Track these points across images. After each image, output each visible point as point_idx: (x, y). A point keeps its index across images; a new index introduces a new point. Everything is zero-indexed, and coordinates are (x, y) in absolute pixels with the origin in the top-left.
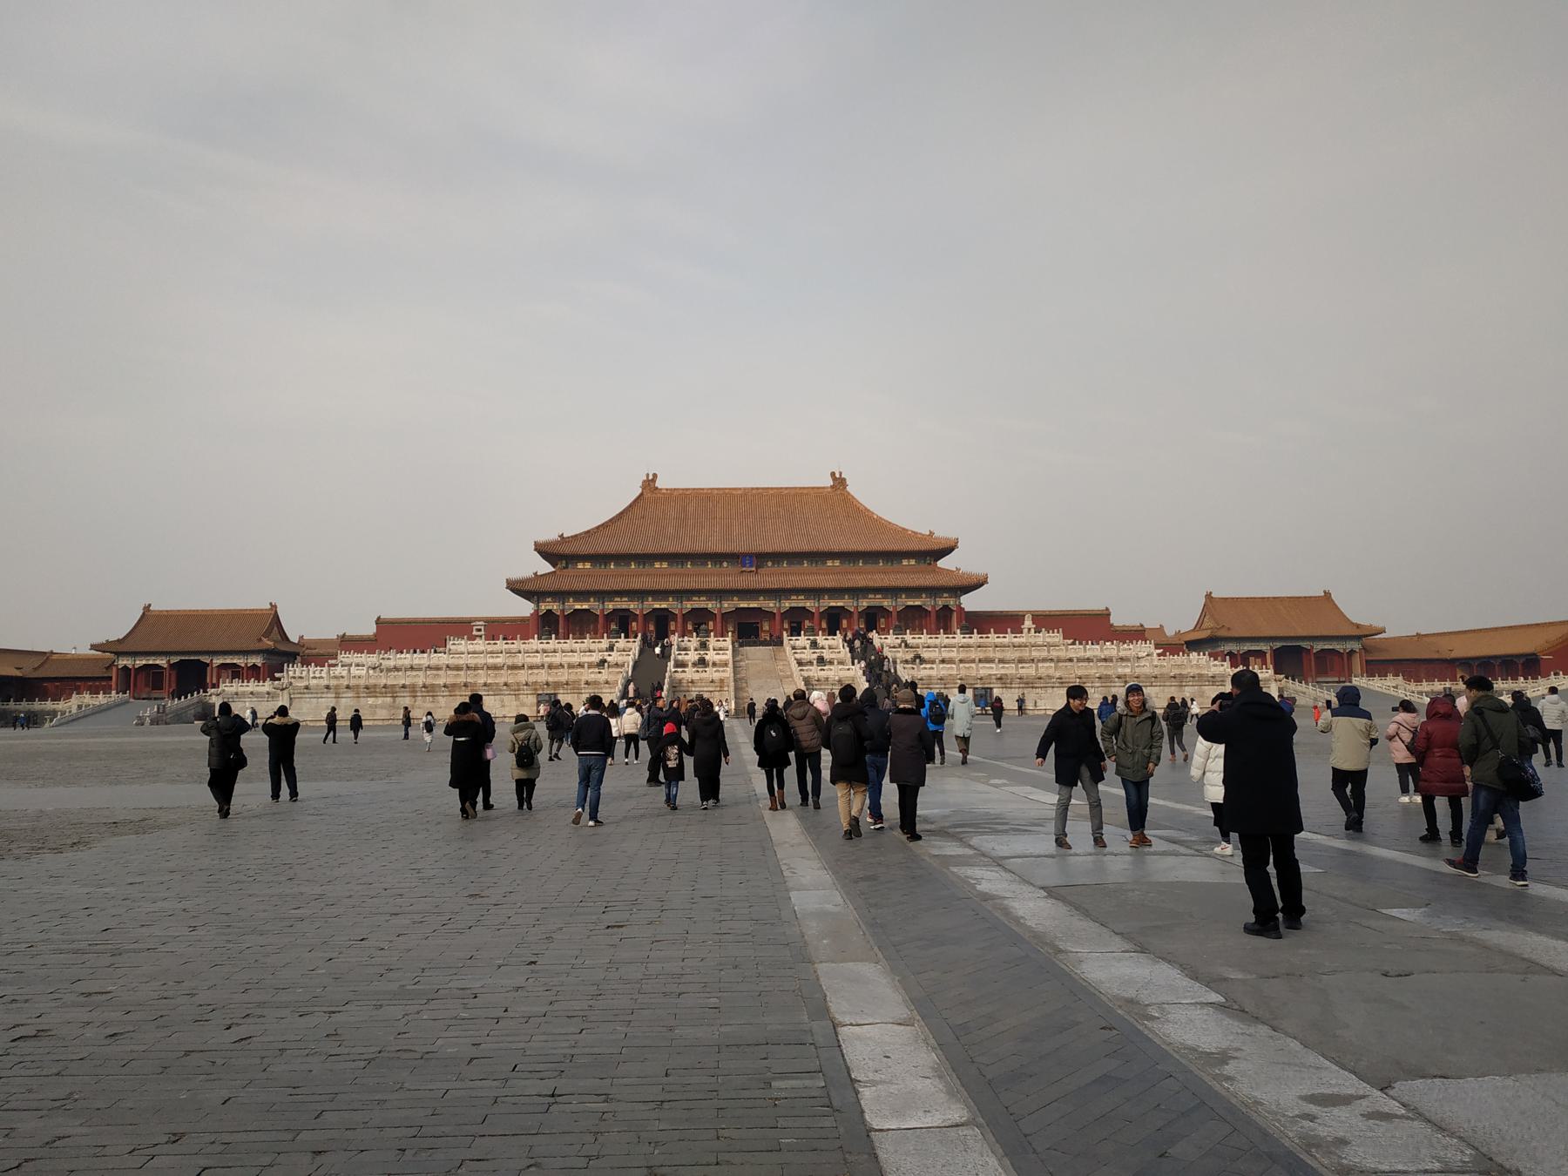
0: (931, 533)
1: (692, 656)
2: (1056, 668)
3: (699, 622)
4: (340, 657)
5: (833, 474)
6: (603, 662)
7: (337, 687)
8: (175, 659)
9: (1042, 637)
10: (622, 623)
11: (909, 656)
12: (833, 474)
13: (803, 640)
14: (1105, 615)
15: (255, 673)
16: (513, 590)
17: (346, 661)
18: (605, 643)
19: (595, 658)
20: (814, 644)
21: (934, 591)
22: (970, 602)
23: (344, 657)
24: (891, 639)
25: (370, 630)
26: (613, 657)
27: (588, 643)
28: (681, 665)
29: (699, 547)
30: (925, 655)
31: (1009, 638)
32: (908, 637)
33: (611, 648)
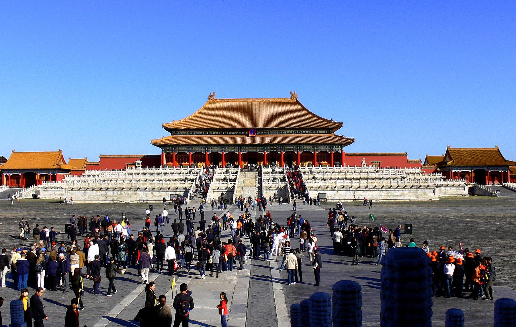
0: (332, 120)
1: (223, 176)
2: (367, 182)
3: (232, 159)
4: (86, 172)
5: (291, 93)
6: (185, 180)
7: (85, 188)
8: (24, 172)
9: (370, 168)
10: (198, 158)
12: (291, 93)
13: (270, 169)
16: (153, 144)
17: (89, 174)
19: (182, 177)
20: (273, 172)
21: (331, 145)
23: (87, 172)
24: (307, 169)
25: (97, 160)
26: (192, 177)
29: (231, 126)
30: (318, 176)
31: (356, 169)
32: (314, 169)
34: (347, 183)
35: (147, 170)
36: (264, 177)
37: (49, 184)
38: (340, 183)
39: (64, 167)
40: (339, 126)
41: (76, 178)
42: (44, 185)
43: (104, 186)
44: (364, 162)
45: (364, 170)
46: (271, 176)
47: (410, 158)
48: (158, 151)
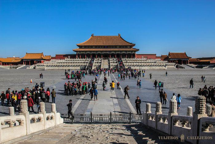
1: (97, 61)
3: (99, 56)
8: (30, 60)
11: (126, 62)
13: (112, 59)
14: (156, 55)
15: (41, 62)
18: (85, 59)
20: (113, 60)
21: (132, 51)
22: (137, 53)
23: (52, 60)
25: (54, 56)
26: (87, 61)
27: (84, 59)
28: (95, 63)
30: (128, 61)
33: (86, 60)
34: (137, 64)
35: (72, 59)
36: (110, 61)
37: (39, 64)
38: (135, 64)
39: (43, 58)
40: (134, 45)
41: (48, 62)
42: (37, 64)
43: (58, 64)
44: (143, 57)
45: (143, 60)
46: (113, 61)
47: (157, 56)
48: (75, 53)
